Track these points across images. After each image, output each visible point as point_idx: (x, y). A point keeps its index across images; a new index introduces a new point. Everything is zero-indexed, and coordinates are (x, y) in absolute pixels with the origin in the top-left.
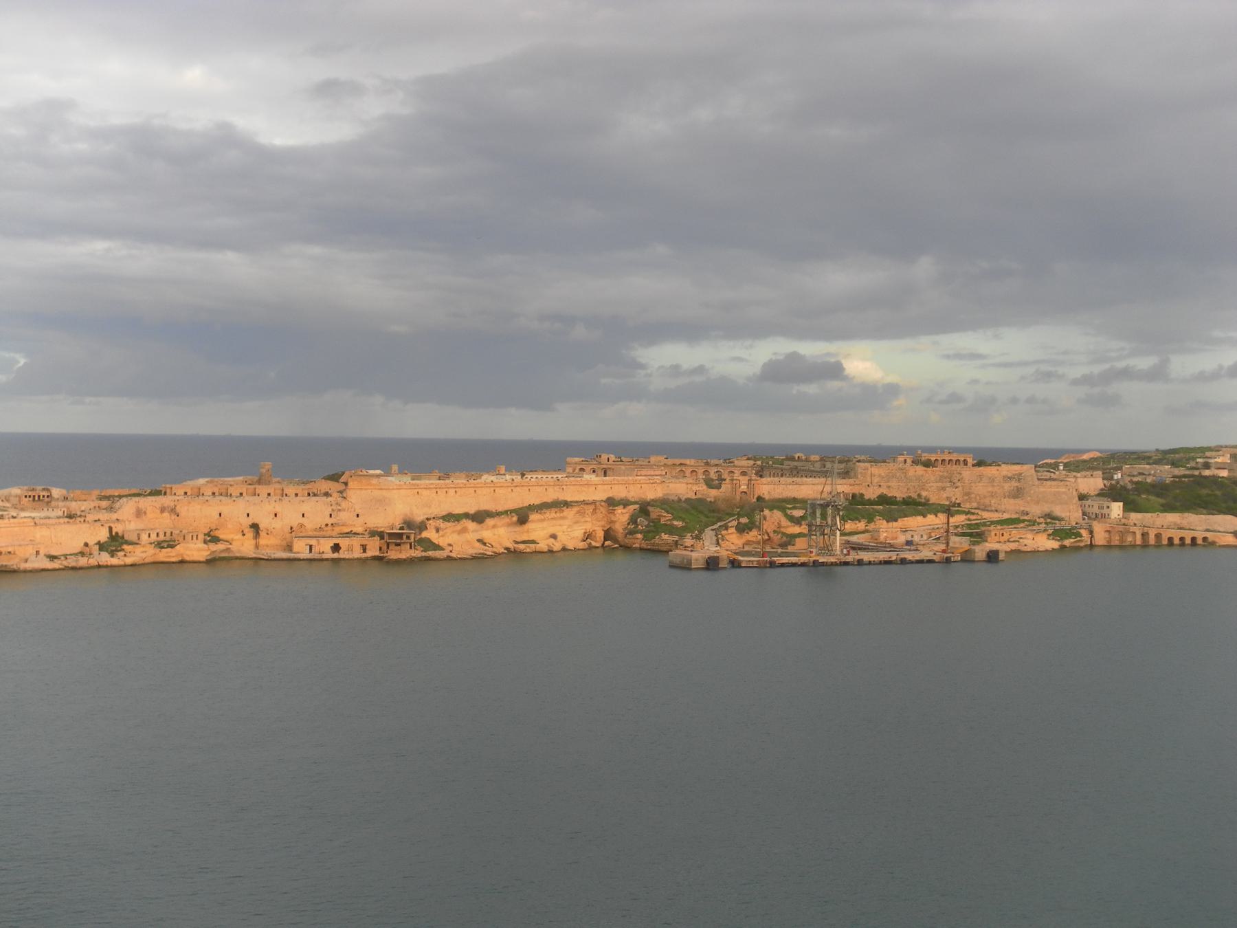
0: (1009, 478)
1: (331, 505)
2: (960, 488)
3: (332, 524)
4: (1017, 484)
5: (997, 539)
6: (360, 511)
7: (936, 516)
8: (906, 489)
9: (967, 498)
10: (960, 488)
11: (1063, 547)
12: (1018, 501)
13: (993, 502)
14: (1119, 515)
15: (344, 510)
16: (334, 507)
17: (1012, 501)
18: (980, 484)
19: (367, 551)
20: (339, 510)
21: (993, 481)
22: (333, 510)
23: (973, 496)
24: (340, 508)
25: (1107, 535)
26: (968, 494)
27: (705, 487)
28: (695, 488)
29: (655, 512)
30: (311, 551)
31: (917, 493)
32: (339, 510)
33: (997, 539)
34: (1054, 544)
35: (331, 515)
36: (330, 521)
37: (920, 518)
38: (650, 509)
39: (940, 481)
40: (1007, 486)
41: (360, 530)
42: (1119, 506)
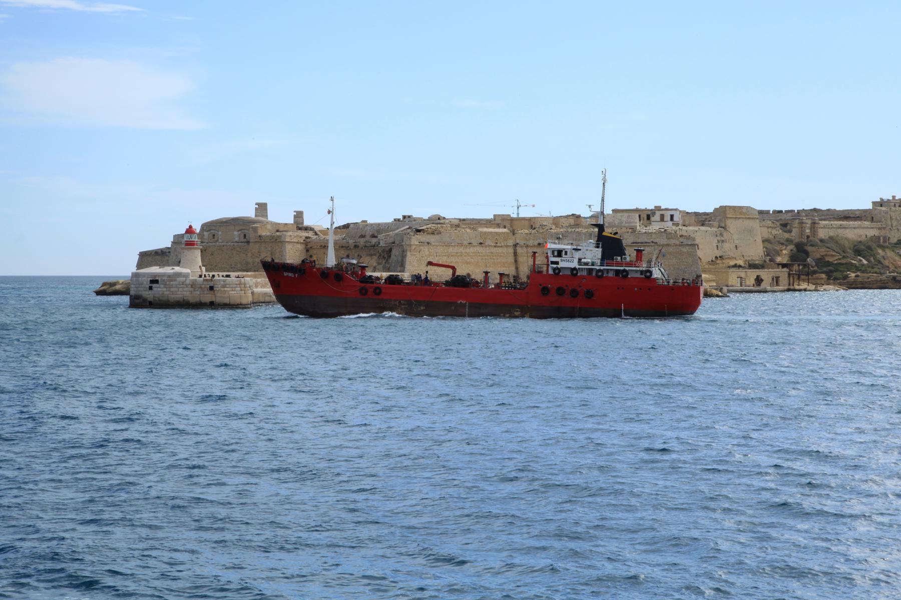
1: (717, 236)
3: (720, 257)
6: (737, 242)
15: (726, 242)
16: (719, 239)
19: (780, 283)
20: (723, 241)
22: (718, 242)
24: (723, 239)
27: (781, 231)
28: (774, 232)
29: (816, 253)
30: (741, 286)
32: (723, 241)
35: (717, 246)
36: (718, 253)
38: (809, 249)
41: (740, 262)
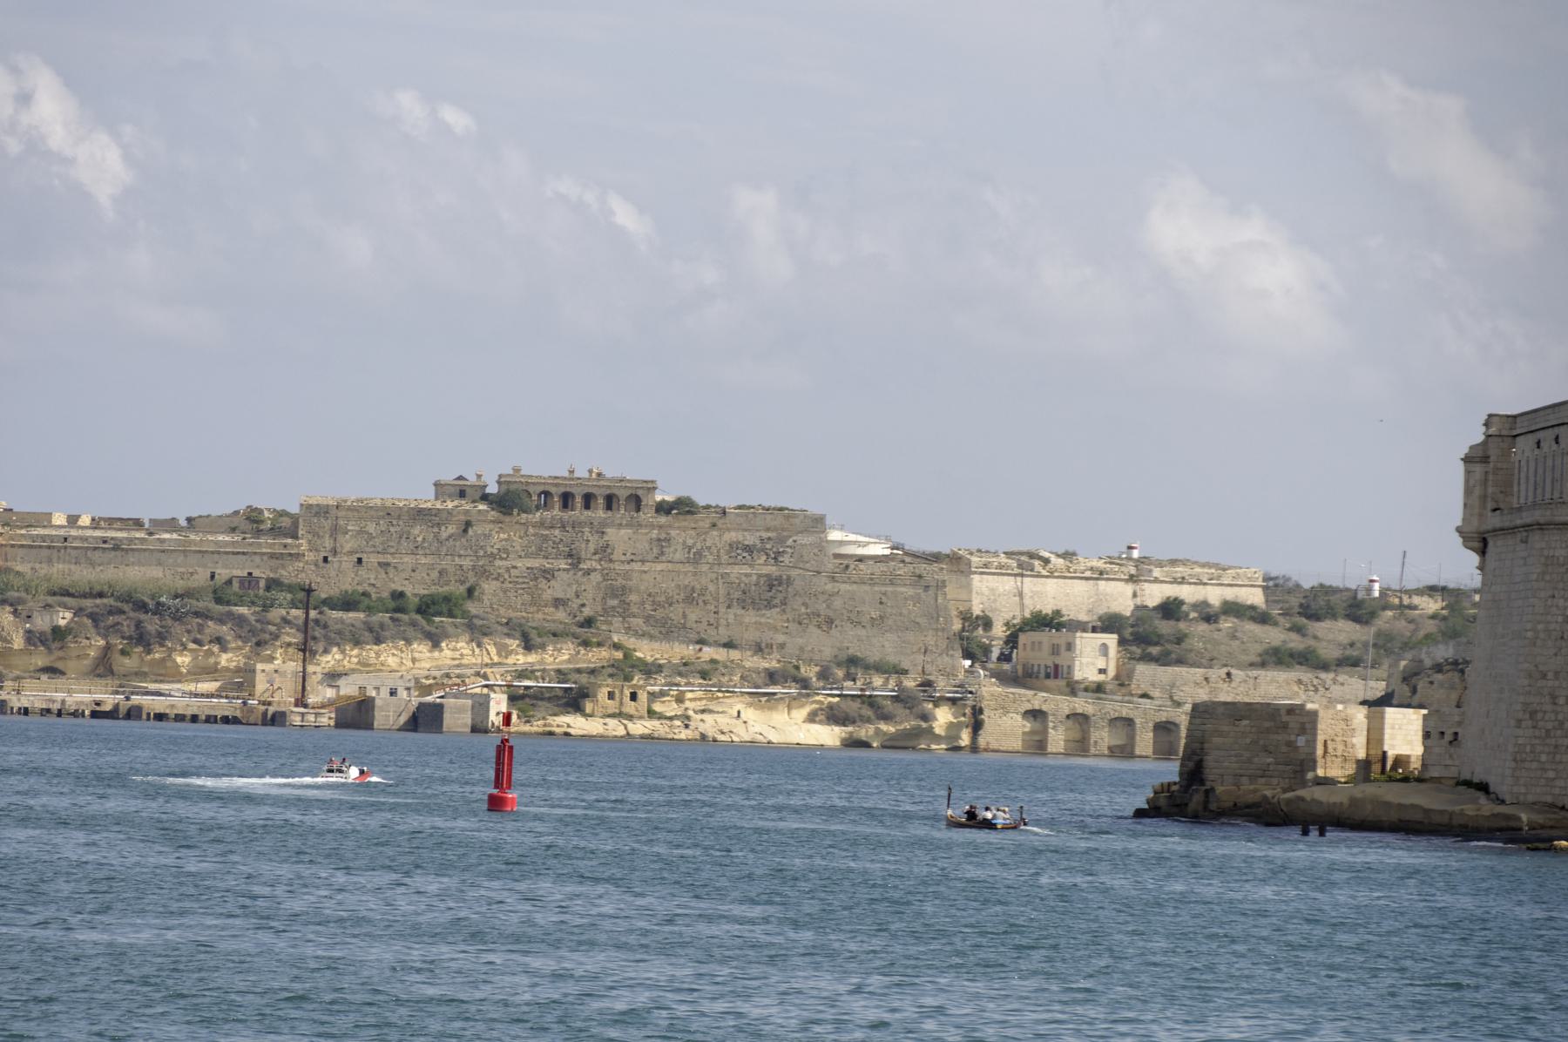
0: (749, 549)
2: (596, 577)
4: (771, 569)
5: (612, 706)
7: (479, 645)
8: (435, 574)
9: (615, 602)
10: (596, 577)
11: (853, 743)
12: (772, 616)
13: (692, 617)
14: (1102, 671)
17: (750, 617)
18: (659, 567)
21: (699, 554)
23: (633, 598)
25: (1028, 726)
26: (614, 592)
31: (468, 585)
33: (612, 706)
34: (828, 735)
37: (421, 649)
39: (540, 552)
40: (736, 571)
42: (1104, 647)
